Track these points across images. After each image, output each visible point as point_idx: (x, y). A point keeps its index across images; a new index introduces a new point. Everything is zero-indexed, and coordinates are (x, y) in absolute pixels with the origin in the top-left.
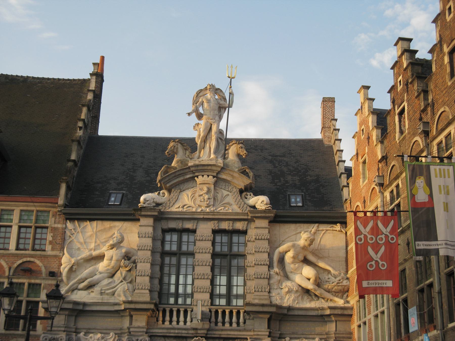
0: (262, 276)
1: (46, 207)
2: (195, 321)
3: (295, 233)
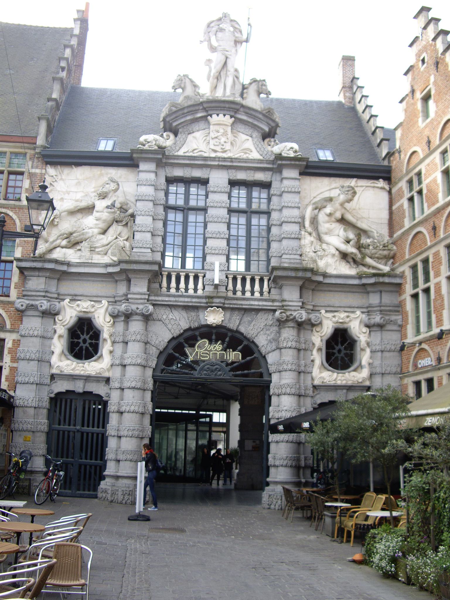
2: (207, 288)
3: (328, 188)
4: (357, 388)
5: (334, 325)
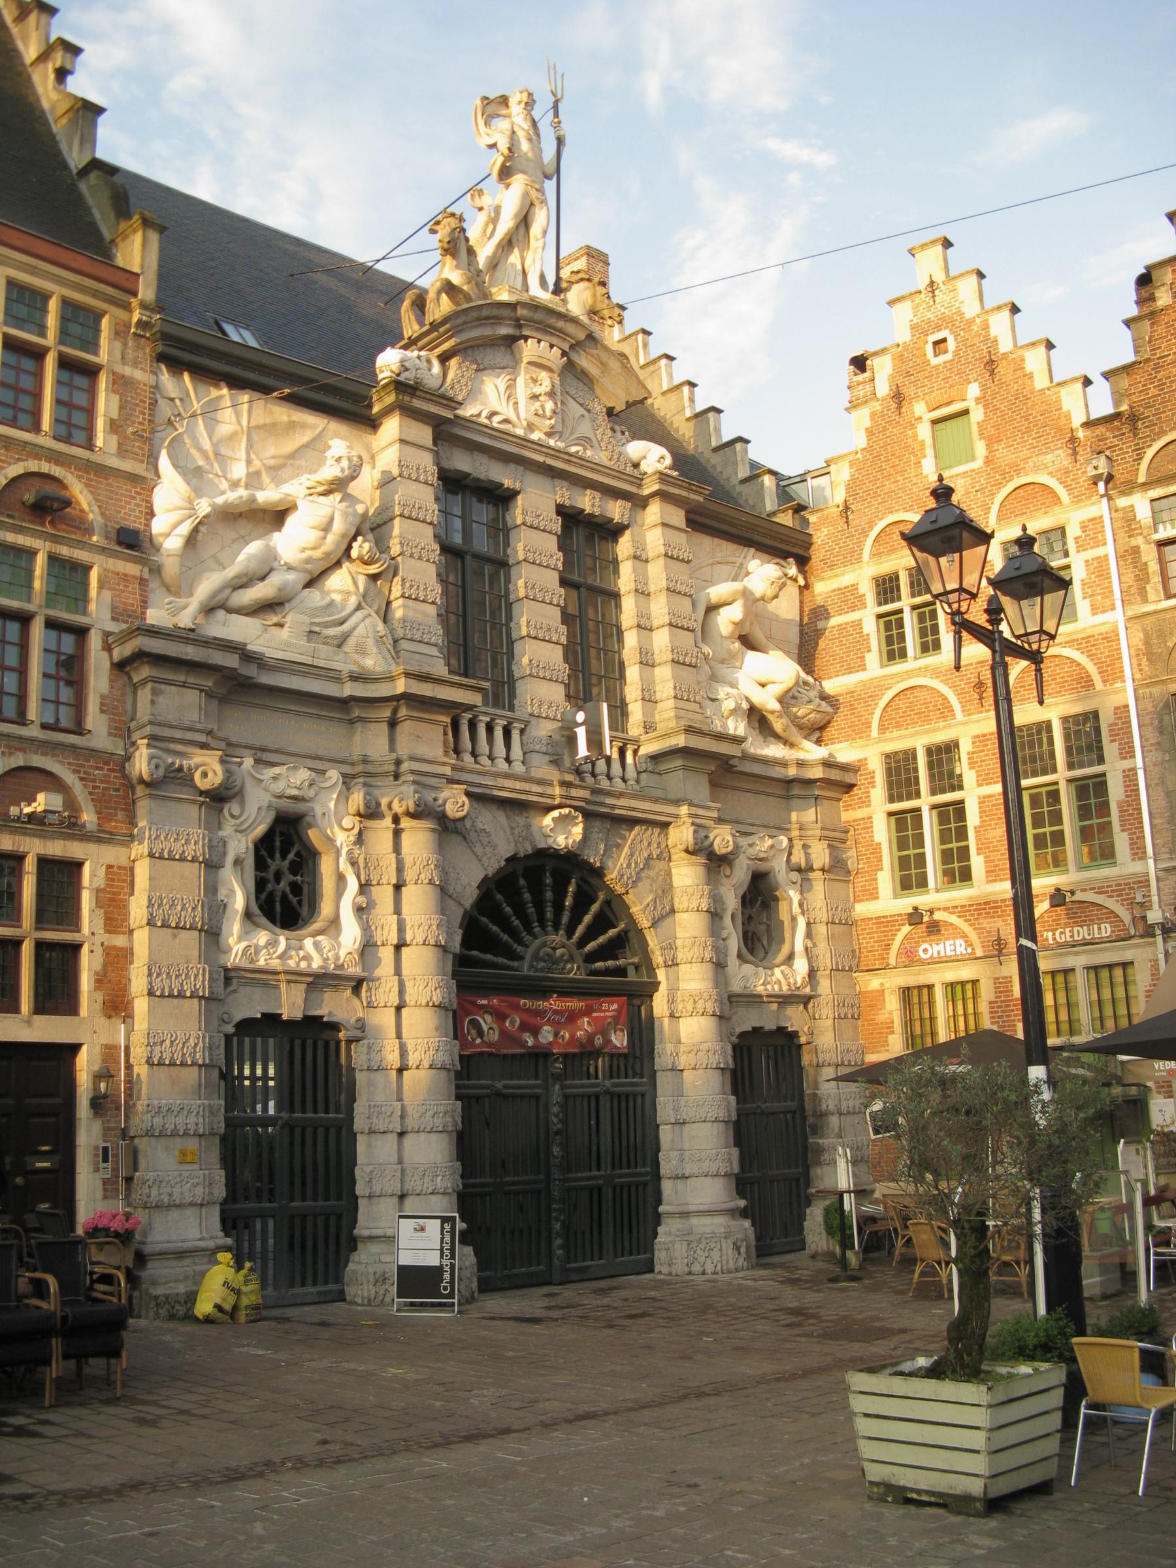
1: (95, 294)
3: (711, 561)
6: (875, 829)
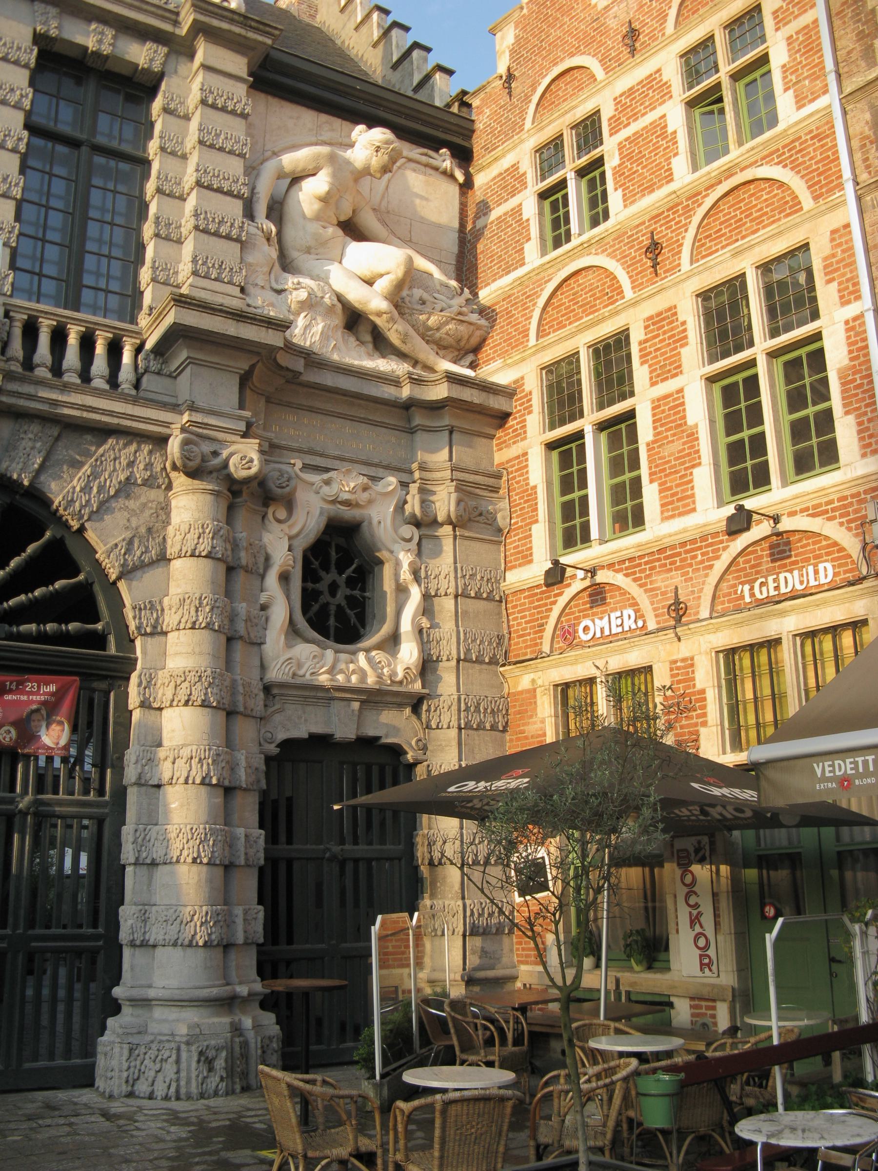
0: (224, 230)
4: (389, 699)
5: (326, 506)
6: (530, 469)
